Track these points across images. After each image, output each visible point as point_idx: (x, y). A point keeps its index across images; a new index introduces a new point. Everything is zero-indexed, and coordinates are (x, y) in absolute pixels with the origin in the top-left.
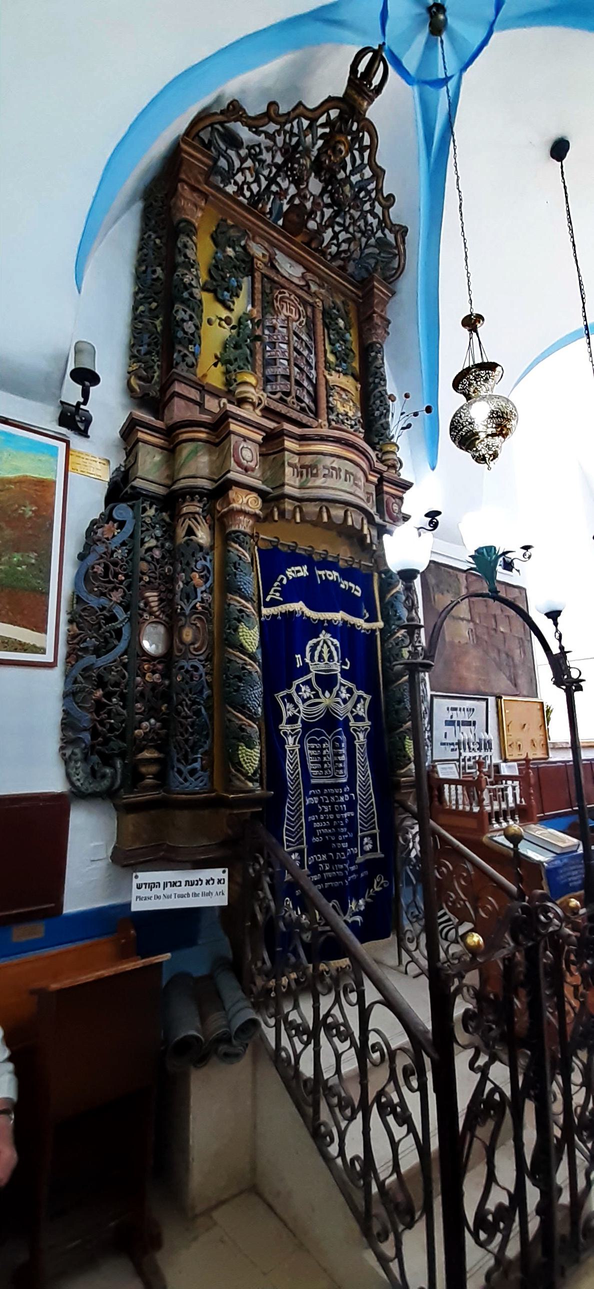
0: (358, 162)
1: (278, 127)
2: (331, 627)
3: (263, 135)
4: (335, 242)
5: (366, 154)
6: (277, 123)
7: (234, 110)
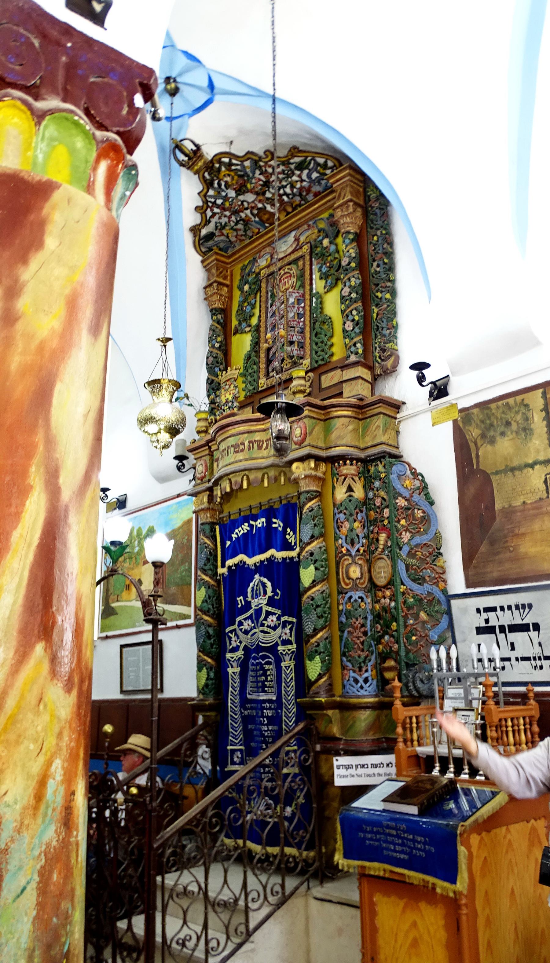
0: (239, 167)
1: (209, 210)
3: (211, 219)
4: (291, 197)
5: (234, 161)
6: (206, 210)
7: (195, 230)
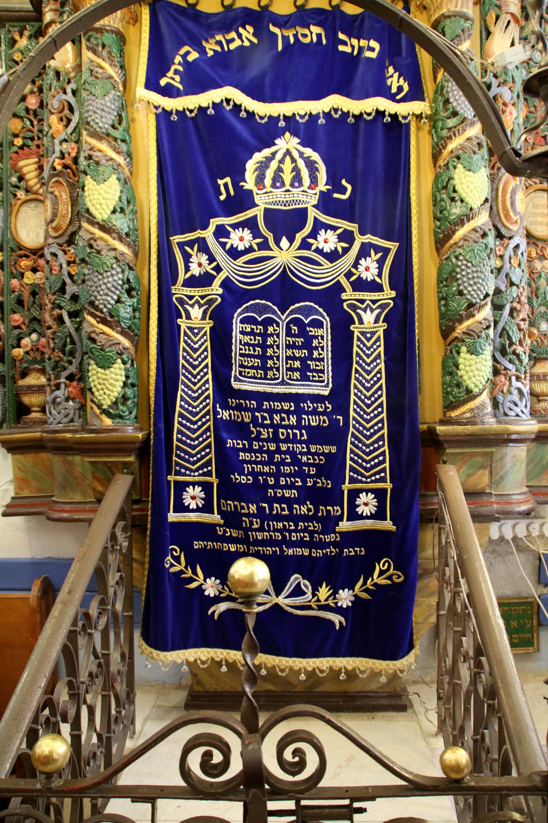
2: (291, 124)
